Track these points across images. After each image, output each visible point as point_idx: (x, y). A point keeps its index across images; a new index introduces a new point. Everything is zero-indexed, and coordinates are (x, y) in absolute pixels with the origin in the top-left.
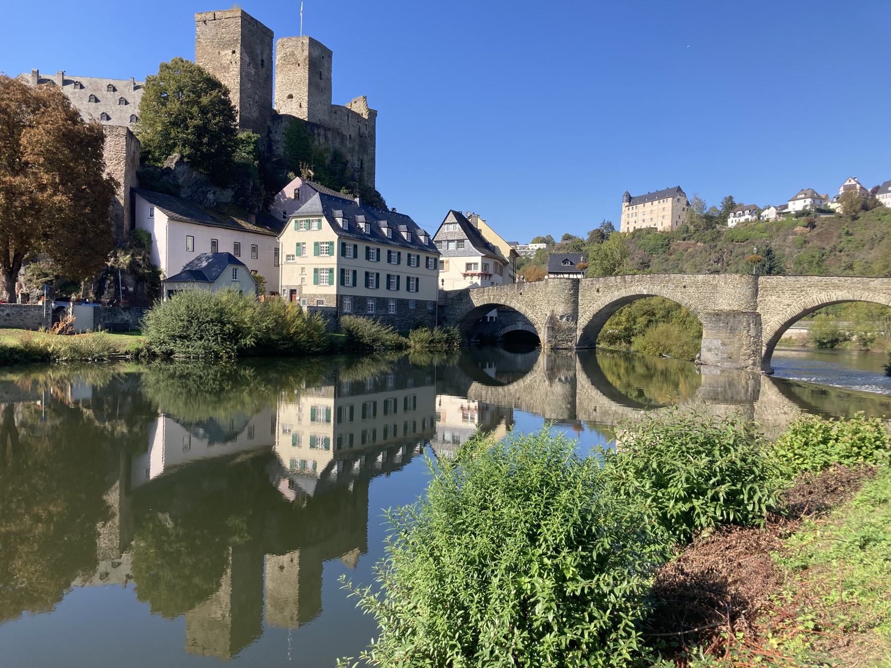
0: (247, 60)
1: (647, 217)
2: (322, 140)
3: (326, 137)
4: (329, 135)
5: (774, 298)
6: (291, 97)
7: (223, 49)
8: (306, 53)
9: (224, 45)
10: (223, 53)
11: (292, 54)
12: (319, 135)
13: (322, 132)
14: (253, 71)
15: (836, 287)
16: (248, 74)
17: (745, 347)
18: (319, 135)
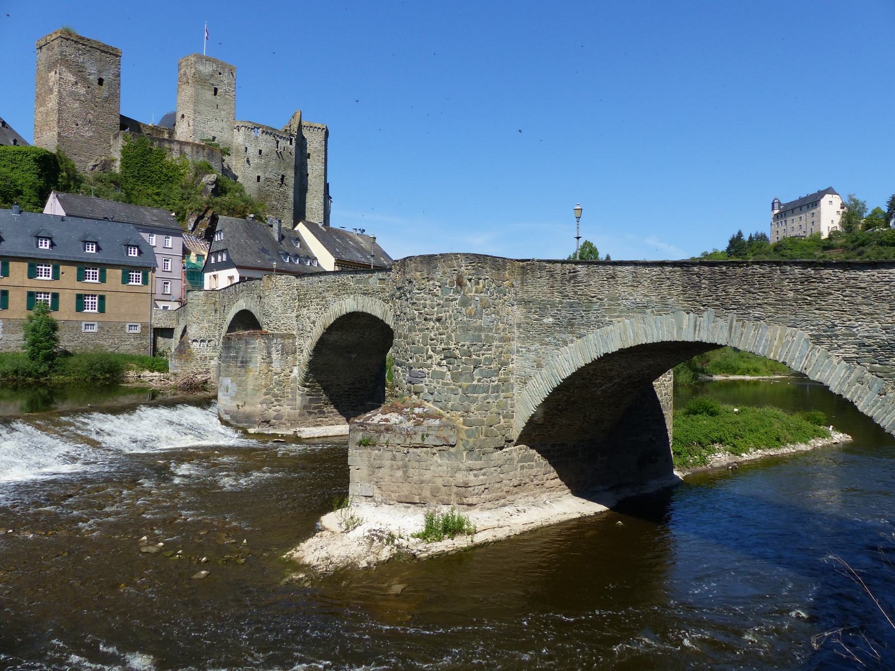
0: (73, 79)
1: (796, 225)
2: (175, 156)
3: (181, 152)
4: (188, 150)
5: (304, 311)
6: (183, 116)
7: (50, 72)
8: (193, 71)
9: (50, 67)
10: (50, 75)
11: (185, 74)
12: (171, 150)
13: (176, 147)
14: (82, 91)
15: (344, 289)
16: (73, 94)
17: (264, 390)
18: (171, 150)
